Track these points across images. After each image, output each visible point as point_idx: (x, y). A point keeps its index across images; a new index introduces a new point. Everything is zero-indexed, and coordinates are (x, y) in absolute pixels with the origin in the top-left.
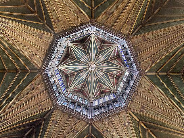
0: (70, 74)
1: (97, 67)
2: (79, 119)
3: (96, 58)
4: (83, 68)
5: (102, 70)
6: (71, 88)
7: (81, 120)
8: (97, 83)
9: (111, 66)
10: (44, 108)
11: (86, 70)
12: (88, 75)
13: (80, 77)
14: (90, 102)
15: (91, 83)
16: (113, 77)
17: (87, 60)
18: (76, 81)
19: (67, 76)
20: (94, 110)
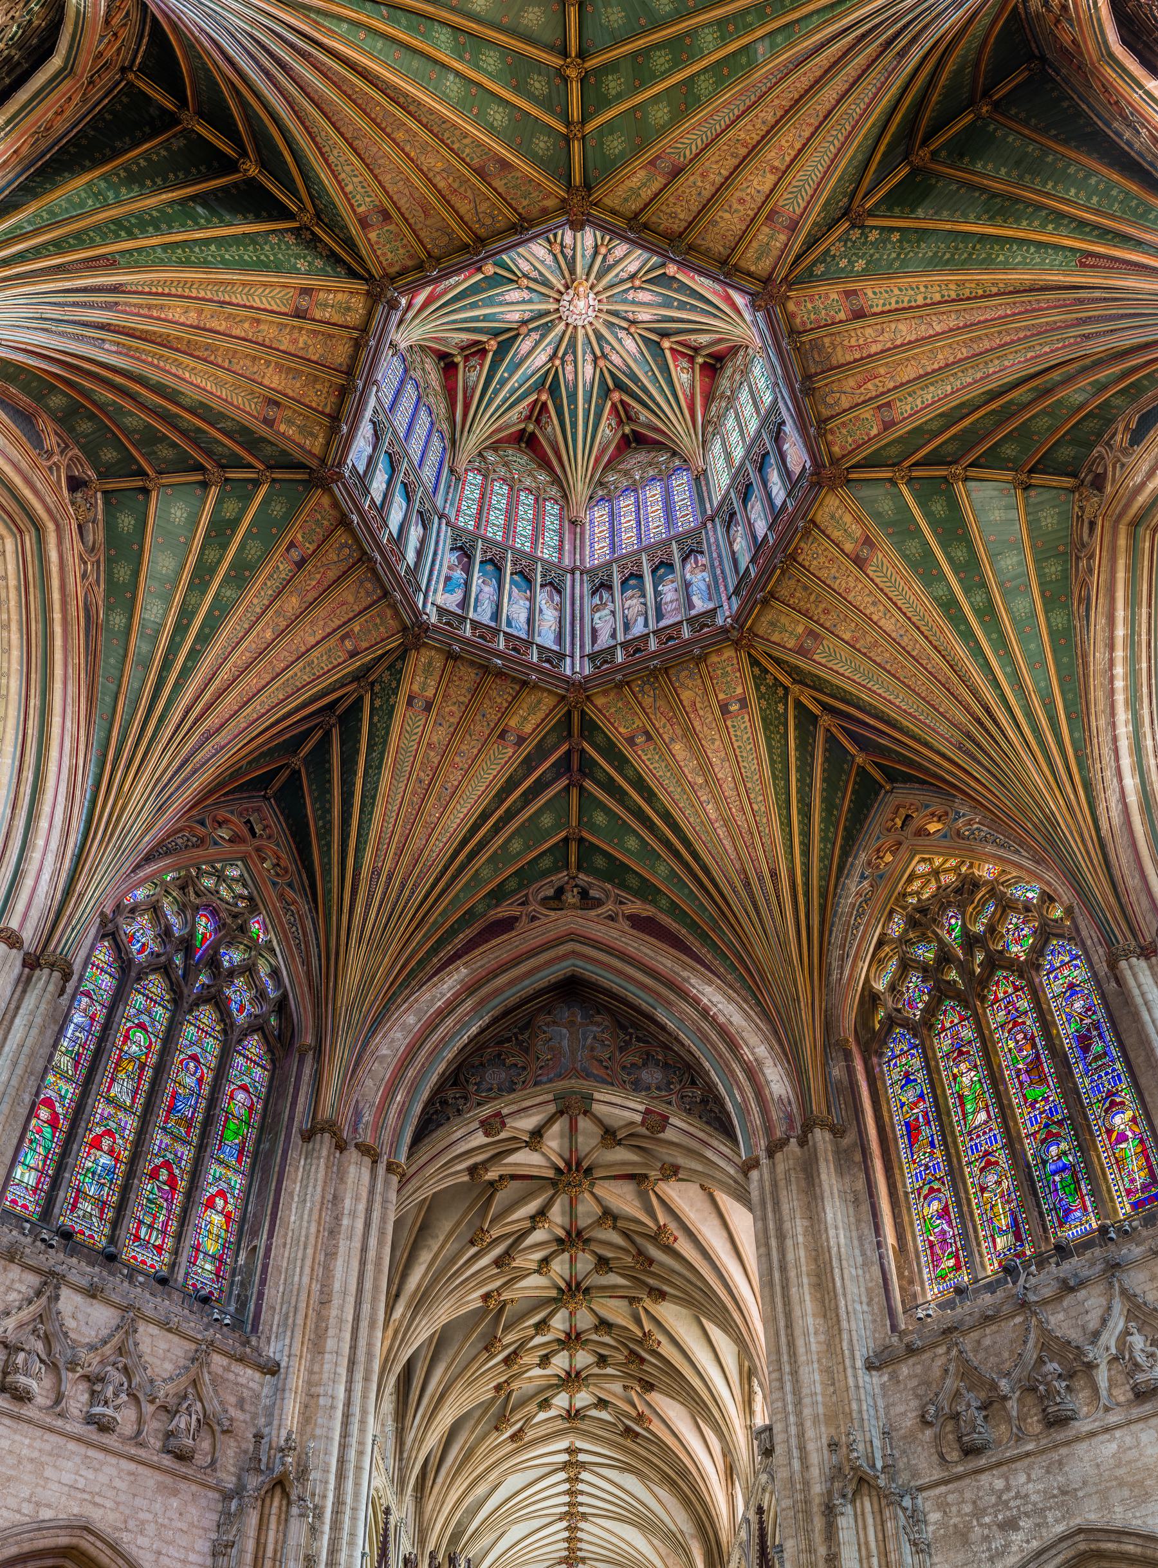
0: (463, 349)
1: (605, 307)
2: (524, 684)
3: (600, 259)
4: (527, 316)
5: (633, 322)
6: (473, 439)
7: (536, 687)
8: (606, 392)
9: (682, 306)
11: (548, 328)
12: (560, 354)
14: (573, 523)
15: (573, 397)
16: (691, 360)
17: (548, 267)
18: (496, 392)
20: (593, 593)
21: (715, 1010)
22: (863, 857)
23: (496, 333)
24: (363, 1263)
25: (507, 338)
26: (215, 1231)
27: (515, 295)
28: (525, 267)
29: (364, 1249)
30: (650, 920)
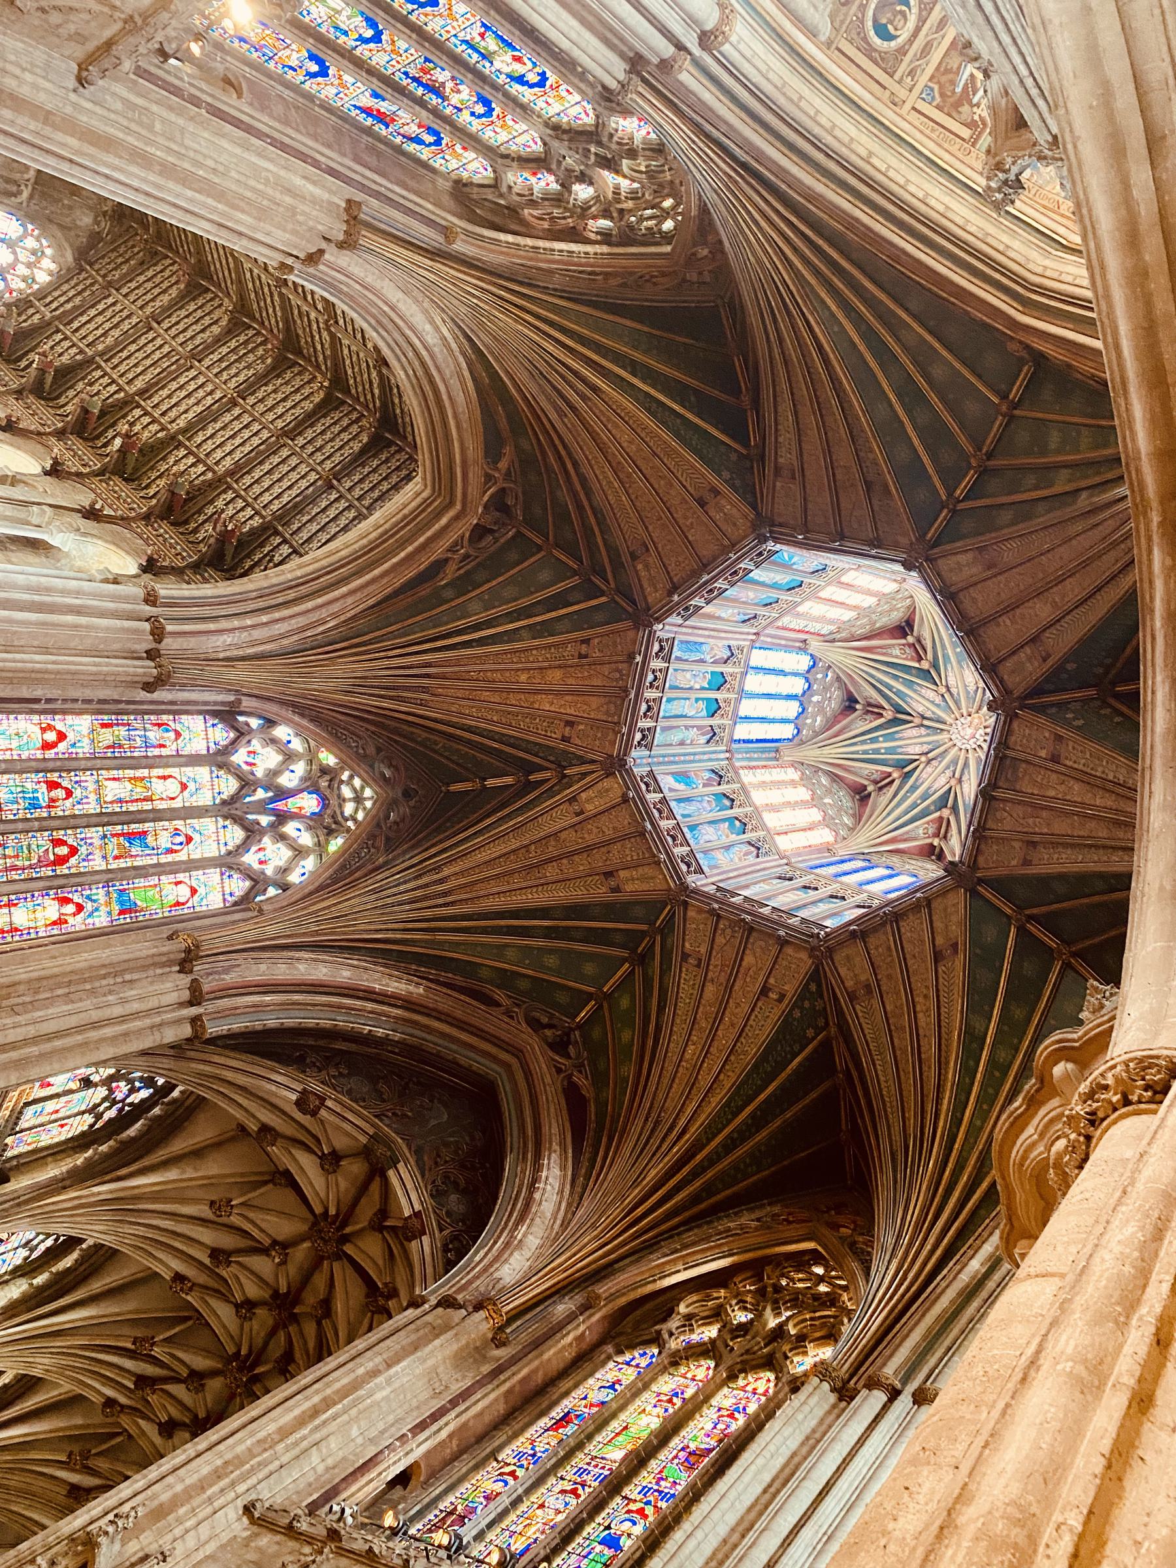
6: (818, 752)
10: (578, 741)
12: (931, 755)
13: (889, 737)
15: (914, 788)
17: (968, 692)
18: (863, 742)
19: (850, 703)
21: (542, 1185)
22: (776, 1209)
23: (899, 710)
24: (80, 1029)
25: (901, 717)
26: (39, 915)
27: (931, 695)
28: (952, 682)
29: (95, 1025)
30: (583, 1101)
